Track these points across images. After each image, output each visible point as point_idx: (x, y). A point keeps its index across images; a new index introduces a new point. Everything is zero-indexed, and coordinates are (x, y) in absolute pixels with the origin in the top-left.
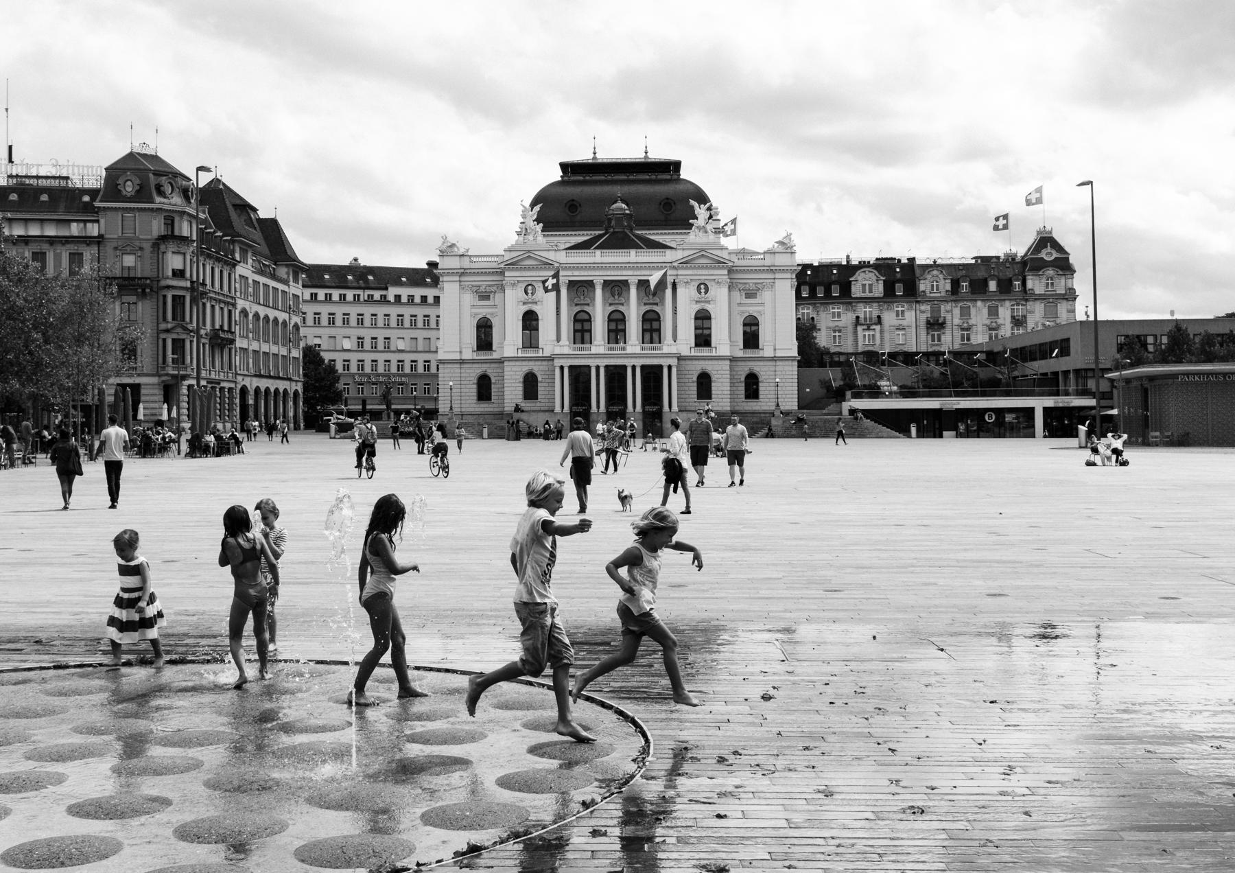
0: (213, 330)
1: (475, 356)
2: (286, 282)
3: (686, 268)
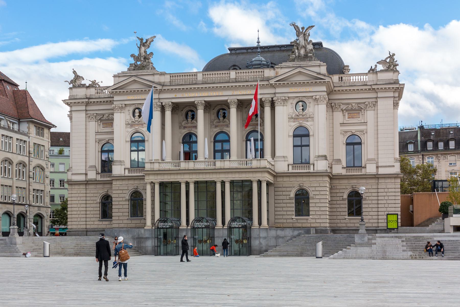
1: (99, 178)
3: (284, 86)
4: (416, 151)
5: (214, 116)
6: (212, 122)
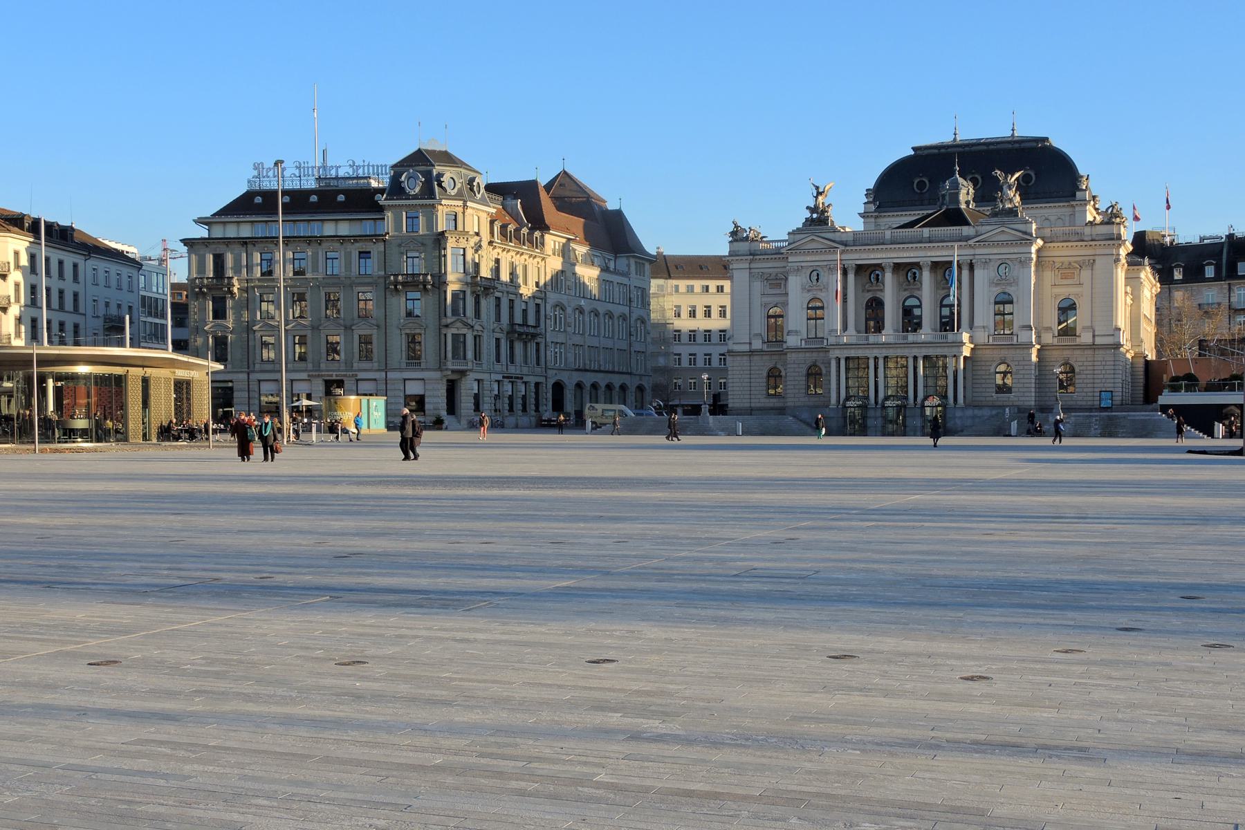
0: (512, 324)
1: (765, 348)
2: (626, 274)
4: (1217, 278)
5: (902, 279)
6: (900, 285)
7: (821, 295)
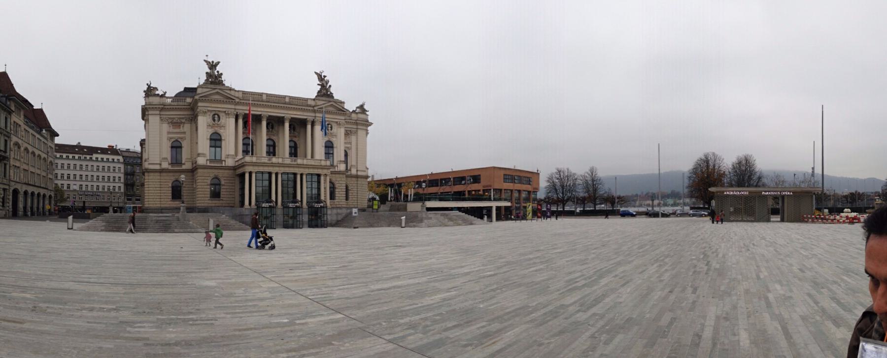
1: (170, 167)
7: (221, 131)
